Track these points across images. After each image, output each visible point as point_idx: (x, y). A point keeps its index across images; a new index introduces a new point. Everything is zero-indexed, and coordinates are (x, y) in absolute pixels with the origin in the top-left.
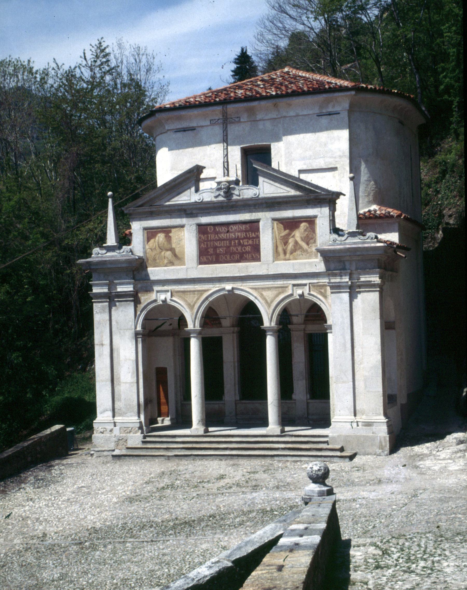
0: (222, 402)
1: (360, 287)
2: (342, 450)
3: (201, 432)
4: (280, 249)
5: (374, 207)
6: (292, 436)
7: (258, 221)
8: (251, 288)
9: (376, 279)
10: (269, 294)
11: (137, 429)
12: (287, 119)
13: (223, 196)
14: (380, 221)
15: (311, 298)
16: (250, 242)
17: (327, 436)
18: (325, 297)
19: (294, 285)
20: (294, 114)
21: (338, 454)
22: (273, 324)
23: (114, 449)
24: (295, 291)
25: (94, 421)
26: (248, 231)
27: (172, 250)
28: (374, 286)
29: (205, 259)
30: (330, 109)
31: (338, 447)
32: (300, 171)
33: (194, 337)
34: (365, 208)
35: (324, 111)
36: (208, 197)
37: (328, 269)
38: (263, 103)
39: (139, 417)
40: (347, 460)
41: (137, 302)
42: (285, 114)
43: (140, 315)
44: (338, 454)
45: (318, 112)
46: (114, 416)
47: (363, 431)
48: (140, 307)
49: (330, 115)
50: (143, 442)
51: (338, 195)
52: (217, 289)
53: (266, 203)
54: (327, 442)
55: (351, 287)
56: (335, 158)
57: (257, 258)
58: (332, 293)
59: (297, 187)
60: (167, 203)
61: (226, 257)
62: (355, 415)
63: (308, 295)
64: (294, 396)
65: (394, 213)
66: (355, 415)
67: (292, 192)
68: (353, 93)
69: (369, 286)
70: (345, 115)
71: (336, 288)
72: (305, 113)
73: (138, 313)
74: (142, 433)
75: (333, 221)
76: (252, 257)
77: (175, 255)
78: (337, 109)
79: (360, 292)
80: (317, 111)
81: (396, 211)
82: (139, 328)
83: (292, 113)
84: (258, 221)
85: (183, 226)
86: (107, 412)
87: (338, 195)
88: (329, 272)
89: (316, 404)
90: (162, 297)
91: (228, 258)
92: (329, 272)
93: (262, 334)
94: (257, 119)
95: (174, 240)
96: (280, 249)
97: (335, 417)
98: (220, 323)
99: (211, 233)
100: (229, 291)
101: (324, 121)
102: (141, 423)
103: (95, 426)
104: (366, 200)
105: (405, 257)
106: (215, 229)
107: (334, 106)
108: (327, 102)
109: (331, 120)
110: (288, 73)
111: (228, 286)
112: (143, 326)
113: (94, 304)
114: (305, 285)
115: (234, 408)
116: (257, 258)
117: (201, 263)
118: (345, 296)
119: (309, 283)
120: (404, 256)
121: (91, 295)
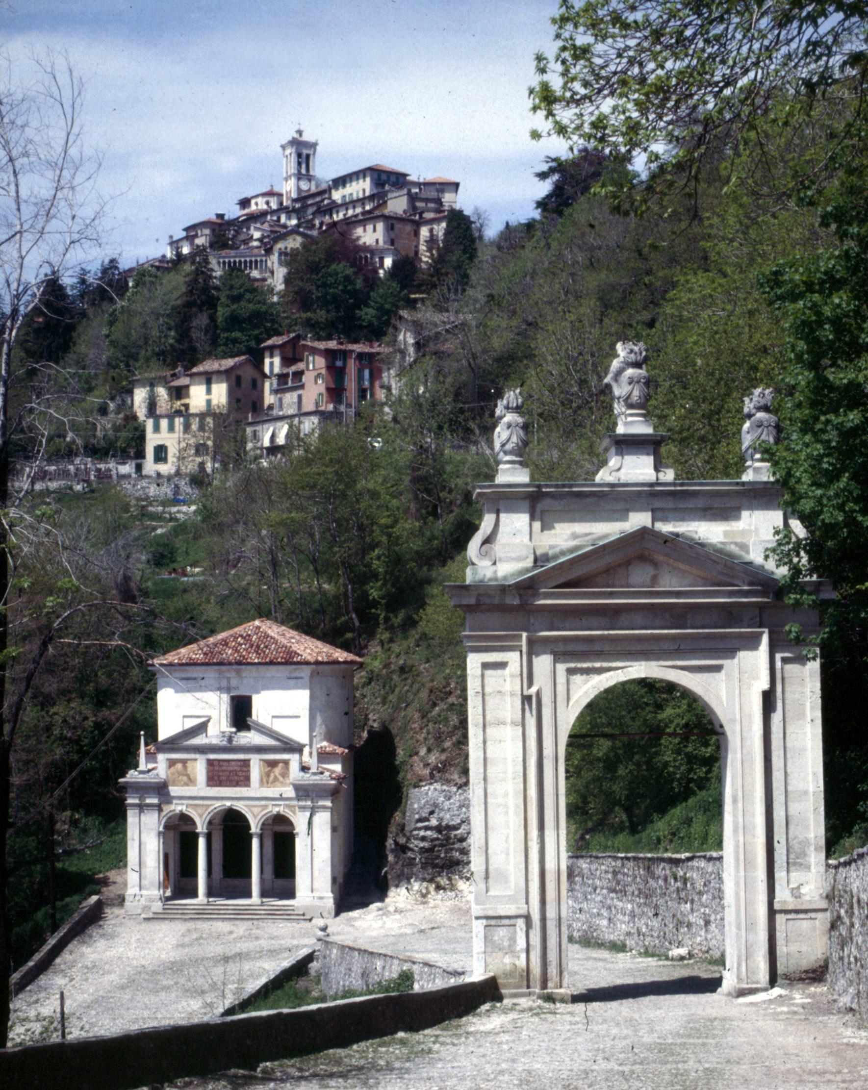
5: (325, 744)
7: (249, 760)
9: (328, 803)
10: (256, 810)
27: (188, 776)
36: (215, 741)
37: (297, 796)
41: (160, 810)
47: (317, 903)
48: (164, 814)
51: (304, 746)
59: (278, 739)
65: (339, 750)
69: (324, 808)
70: (307, 679)
71: (303, 808)
75: (301, 763)
77: (189, 779)
78: (302, 675)
80: (287, 674)
82: (161, 829)
84: (249, 760)
85: (196, 760)
87: (304, 746)
88: (299, 798)
89: (280, 882)
92: (299, 798)
93: (250, 837)
95: (189, 770)
110: (258, 628)
111: (228, 804)
112: (166, 827)
117: (208, 785)
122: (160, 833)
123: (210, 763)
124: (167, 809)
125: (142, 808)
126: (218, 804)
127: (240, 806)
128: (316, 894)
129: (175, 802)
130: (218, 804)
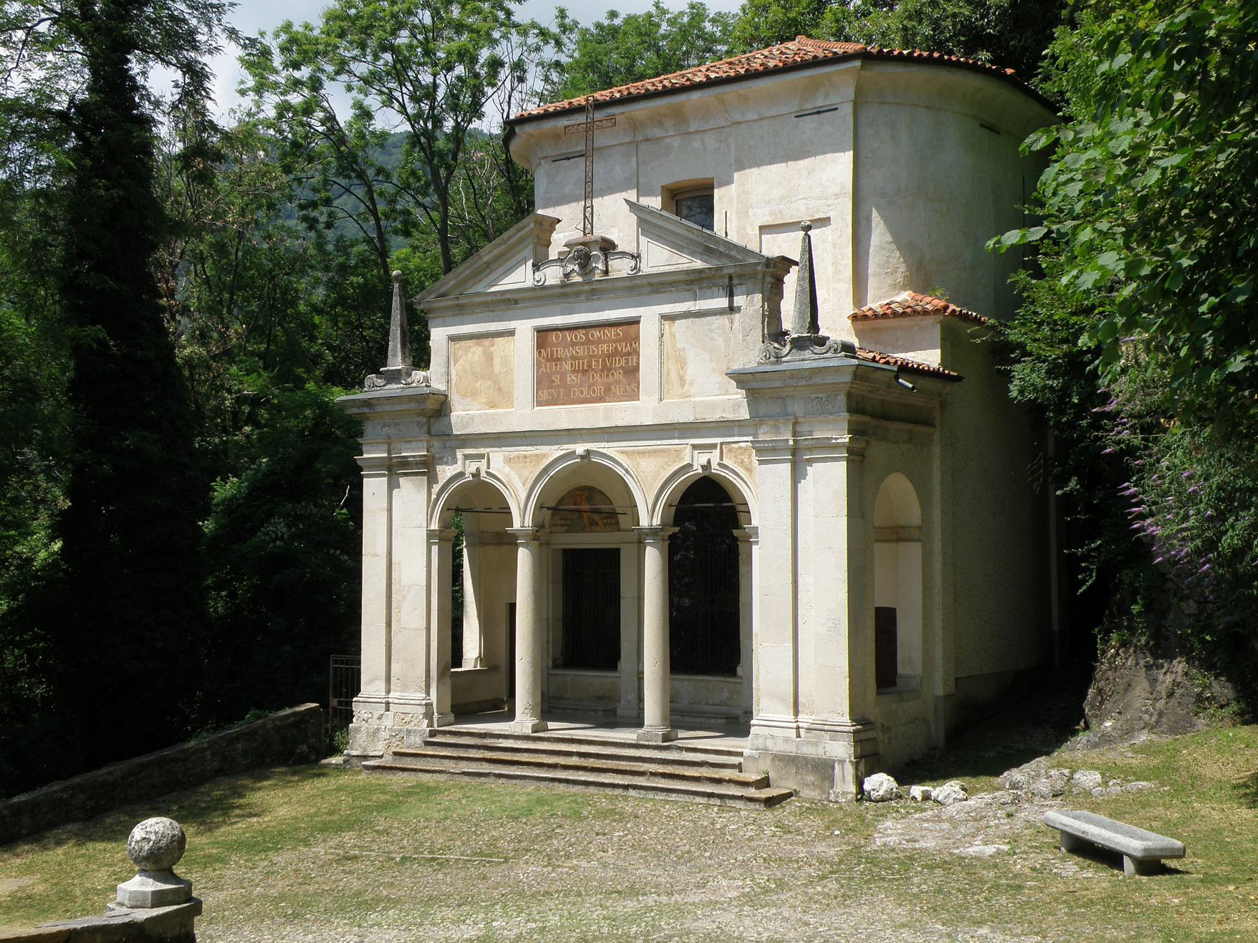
0: (617, 675)
1: (811, 449)
2: (764, 783)
3: (528, 731)
4: (673, 375)
5: (905, 296)
6: (681, 749)
7: (635, 322)
8: (618, 451)
11: (421, 717)
12: (743, 126)
13: (578, 274)
14: (905, 322)
15: (723, 473)
17: (741, 754)
18: (749, 470)
19: (695, 447)
20: (756, 117)
21: (752, 792)
22: (657, 521)
23: (381, 754)
24: (695, 459)
25: (354, 699)
26: (619, 341)
28: (837, 447)
29: (544, 395)
30: (820, 102)
31: (753, 777)
32: (764, 229)
33: (523, 545)
34: (885, 298)
35: (808, 106)
36: (552, 275)
38: (696, 96)
39: (428, 694)
40: (762, 807)
42: (738, 117)
43: (437, 499)
44: (752, 792)
45: (797, 109)
46: (388, 692)
49: (819, 113)
50: (427, 743)
52: (565, 452)
53: (650, 284)
54: (739, 767)
55: (795, 452)
56: (826, 198)
57: (634, 396)
58: (761, 462)
60: (493, 289)
61: (582, 392)
62: (796, 713)
63: (718, 467)
64: (739, 670)
66: (796, 713)
67: (698, 264)
68: (858, 63)
69: (827, 446)
70: (847, 110)
73: (434, 496)
74: (431, 724)
76: (626, 391)
79: (810, 462)
80: (795, 107)
81: (936, 302)
82: (435, 526)
84: (635, 322)
85: (511, 333)
86: (377, 682)
88: (757, 419)
90: (472, 467)
92: (757, 419)
94: (691, 130)
95: (497, 361)
96: (673, 375)
97: (762, 715)
98: (617, 523)
99: (557, 345)
100: (582, 457)
101: (809, 124)
102: (429, 705)
103: (356, 708)
104: (890, 282)
105: (913, 388)
106: (564, 337)
107: (827, 96)
108: (815, 86)
111: (580, 448)
113: (365, 480)
114: (714, 446)
115: (636, 686)
116: (634, 396)
119: (722, 444)
120: (911, 386)
121: (359, 463)
122: (431, 535)
123: (542, 333)
124: (445, 472)
125: (394, 469)
126: (553, 452)
128: (805, 719)
129: (459, 454)
130: (554, 452)
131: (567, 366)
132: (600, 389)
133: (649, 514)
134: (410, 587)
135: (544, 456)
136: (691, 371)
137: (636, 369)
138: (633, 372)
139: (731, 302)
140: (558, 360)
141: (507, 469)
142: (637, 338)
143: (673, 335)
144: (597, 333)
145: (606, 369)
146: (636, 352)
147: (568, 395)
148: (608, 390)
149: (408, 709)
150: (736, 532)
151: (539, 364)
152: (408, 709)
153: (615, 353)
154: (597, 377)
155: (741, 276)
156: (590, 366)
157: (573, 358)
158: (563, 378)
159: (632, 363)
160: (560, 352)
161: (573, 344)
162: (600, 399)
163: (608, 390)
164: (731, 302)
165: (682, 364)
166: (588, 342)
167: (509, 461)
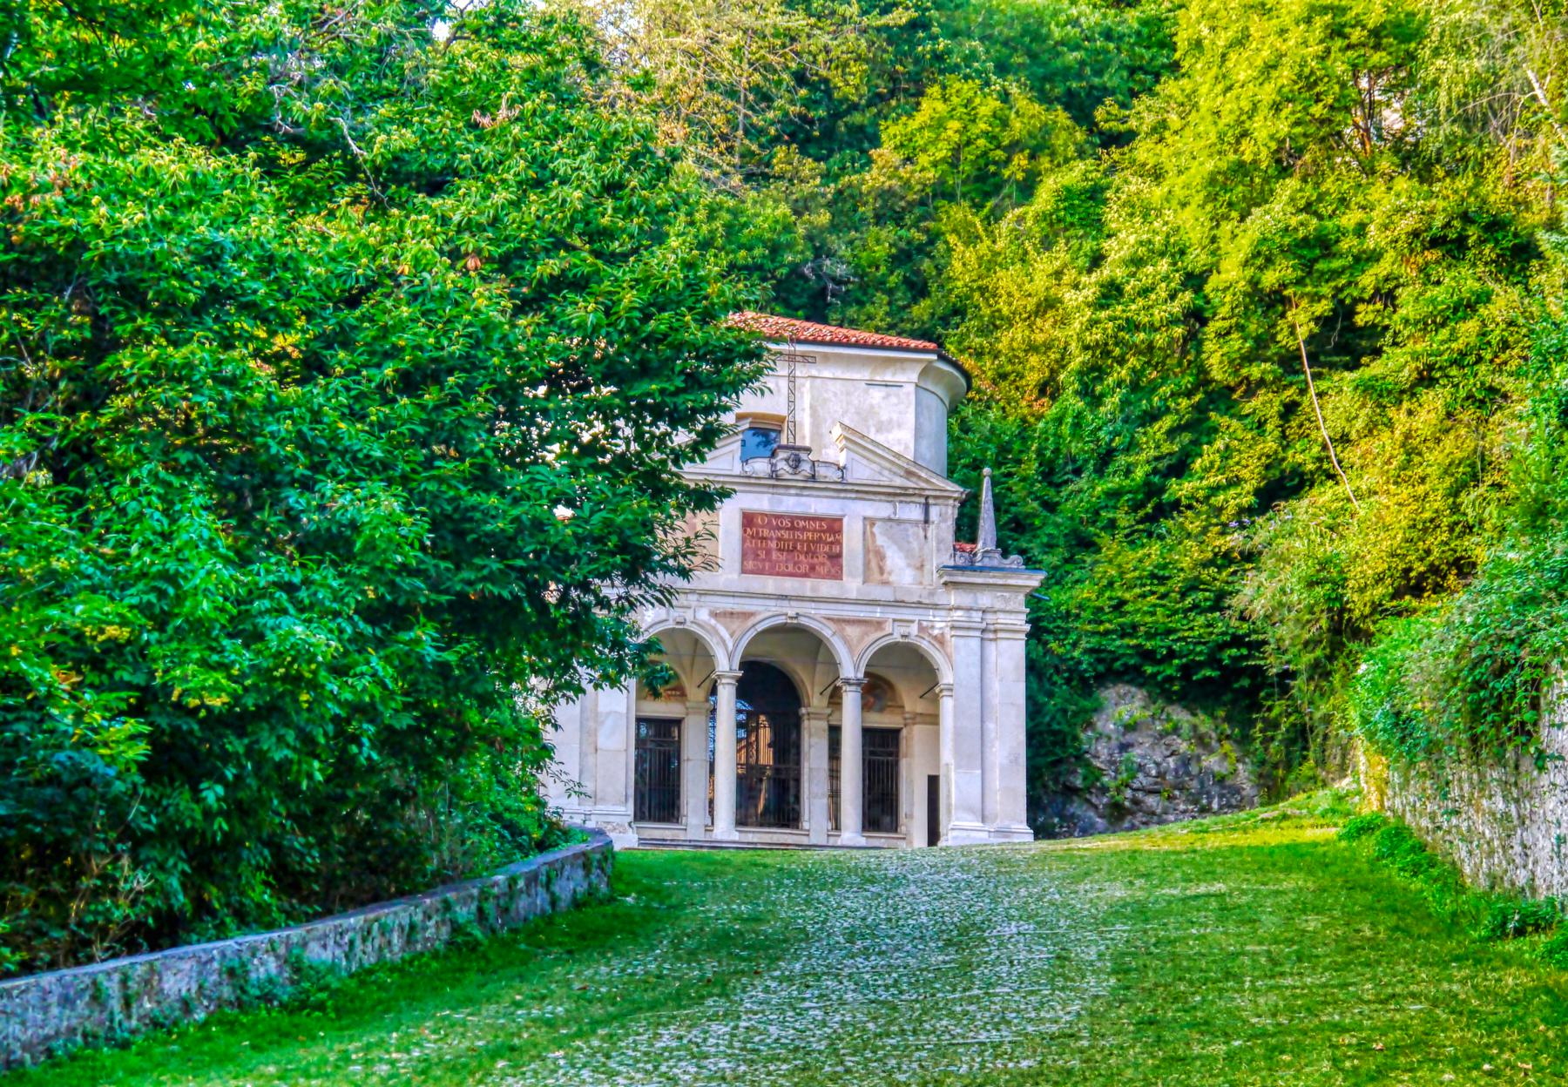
4: (874, 564)
9: (1021, 622)
10: (852, 632)
16: (827, 549)
22: (860, 675)
29: (750, 564)
30: (888, 377)
42: (814, 372)
57: (837, 575)
67: (899, 482)
70: (911, 388)
72: (847, 376)
78: (900, 378)
83: (827, 374)
91: (791, 566)
96: (874, 564)
109: (887, 396)
111: (791, 609)
116: (837, 575)
117: (744, 571)
118: (975, 644)
123: (748, 519)
127: (814, 617)
131: (773, 545)
132: (804, 568)
133: (851, 668)
134: (609, 714)
135: (752, 614)
136: (889, 564)
137: (839, 555)
138: (836, 558)
139: (927, 513)
140: (763, 538)
141: (713, 622)
142: (840, 531)
143: (873, 534)
144: (802, 523)
145: (810, 553)
146: (840, 543)
147: (773, 567)
148: (813, 568)
149: (611, 819)
150: (803, 710)
151: (744, 540)
152: (611, 819)
153: (820, 540)
154: (802, 557)
155: (936, 497)
156: (795, 548)
157: (779, 539)
158: (768, 552)
159: (836, 549)
160: (766, 533)
161: (779, 529)
162: (805, 575)
163: (813, 568)
164: (927, 513)
165: (881, 557)
166: (793, 528)
167: (715, 615)
